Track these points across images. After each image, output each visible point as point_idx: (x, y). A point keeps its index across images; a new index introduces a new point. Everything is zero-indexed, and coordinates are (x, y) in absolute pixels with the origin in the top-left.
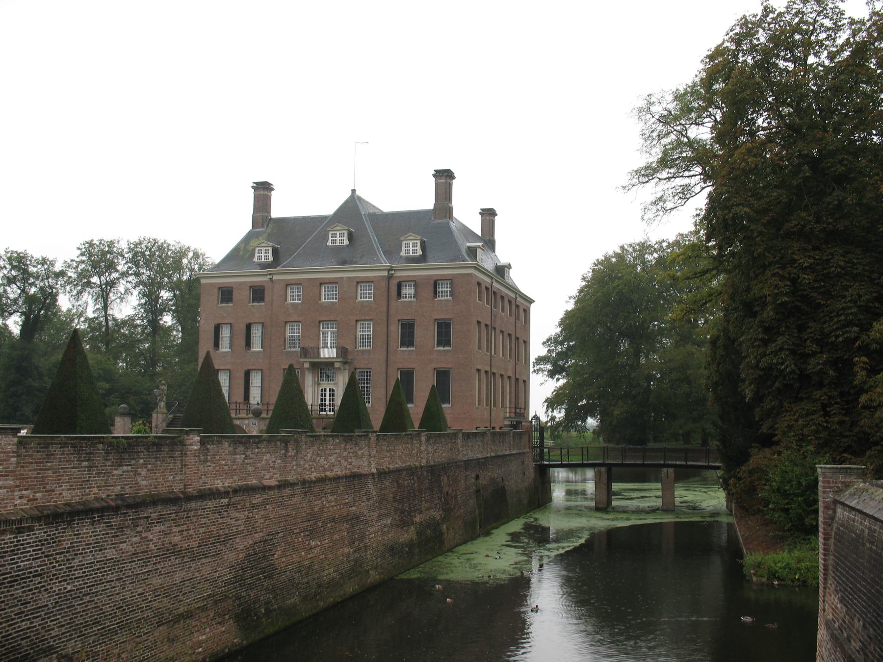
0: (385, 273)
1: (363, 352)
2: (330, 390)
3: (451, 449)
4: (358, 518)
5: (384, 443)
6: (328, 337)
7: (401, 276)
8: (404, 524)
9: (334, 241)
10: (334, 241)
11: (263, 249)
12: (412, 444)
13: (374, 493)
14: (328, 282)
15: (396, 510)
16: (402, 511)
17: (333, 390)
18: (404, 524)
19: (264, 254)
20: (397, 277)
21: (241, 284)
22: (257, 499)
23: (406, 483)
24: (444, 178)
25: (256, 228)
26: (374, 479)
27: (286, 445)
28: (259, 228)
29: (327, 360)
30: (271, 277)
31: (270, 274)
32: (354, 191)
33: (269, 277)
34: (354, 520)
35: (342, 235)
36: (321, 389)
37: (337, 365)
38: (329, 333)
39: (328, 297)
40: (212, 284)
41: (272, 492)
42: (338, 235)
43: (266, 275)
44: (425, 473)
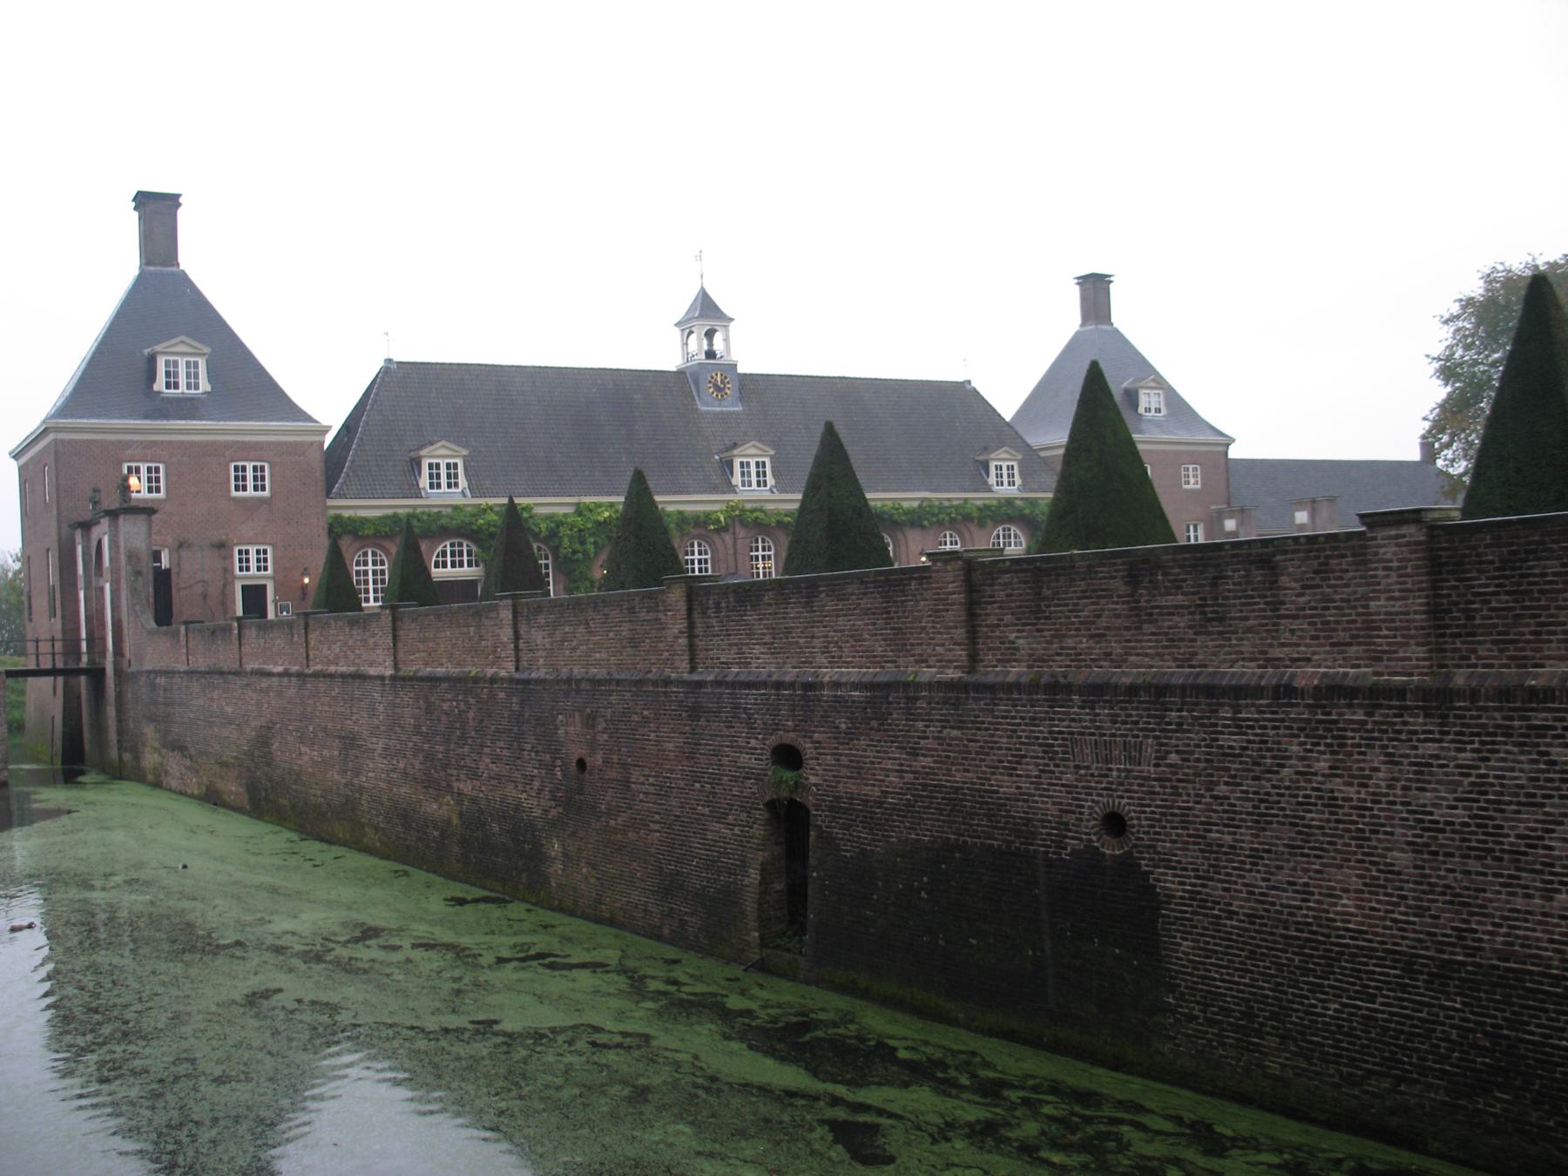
3: (634, 642)
4: (353, 739)
5: (413, 626)
8: (433, 784)
12: (479, 627)
13: (381, 708)
15: (417, 750)
16: (429, 757)
18: (433, 784)
22: (265, 682)
23: (446, 706)
26: (383, 685)
27: (291, 628)
34: (350, 742)
41: (274, 679)
44: (502, 695)
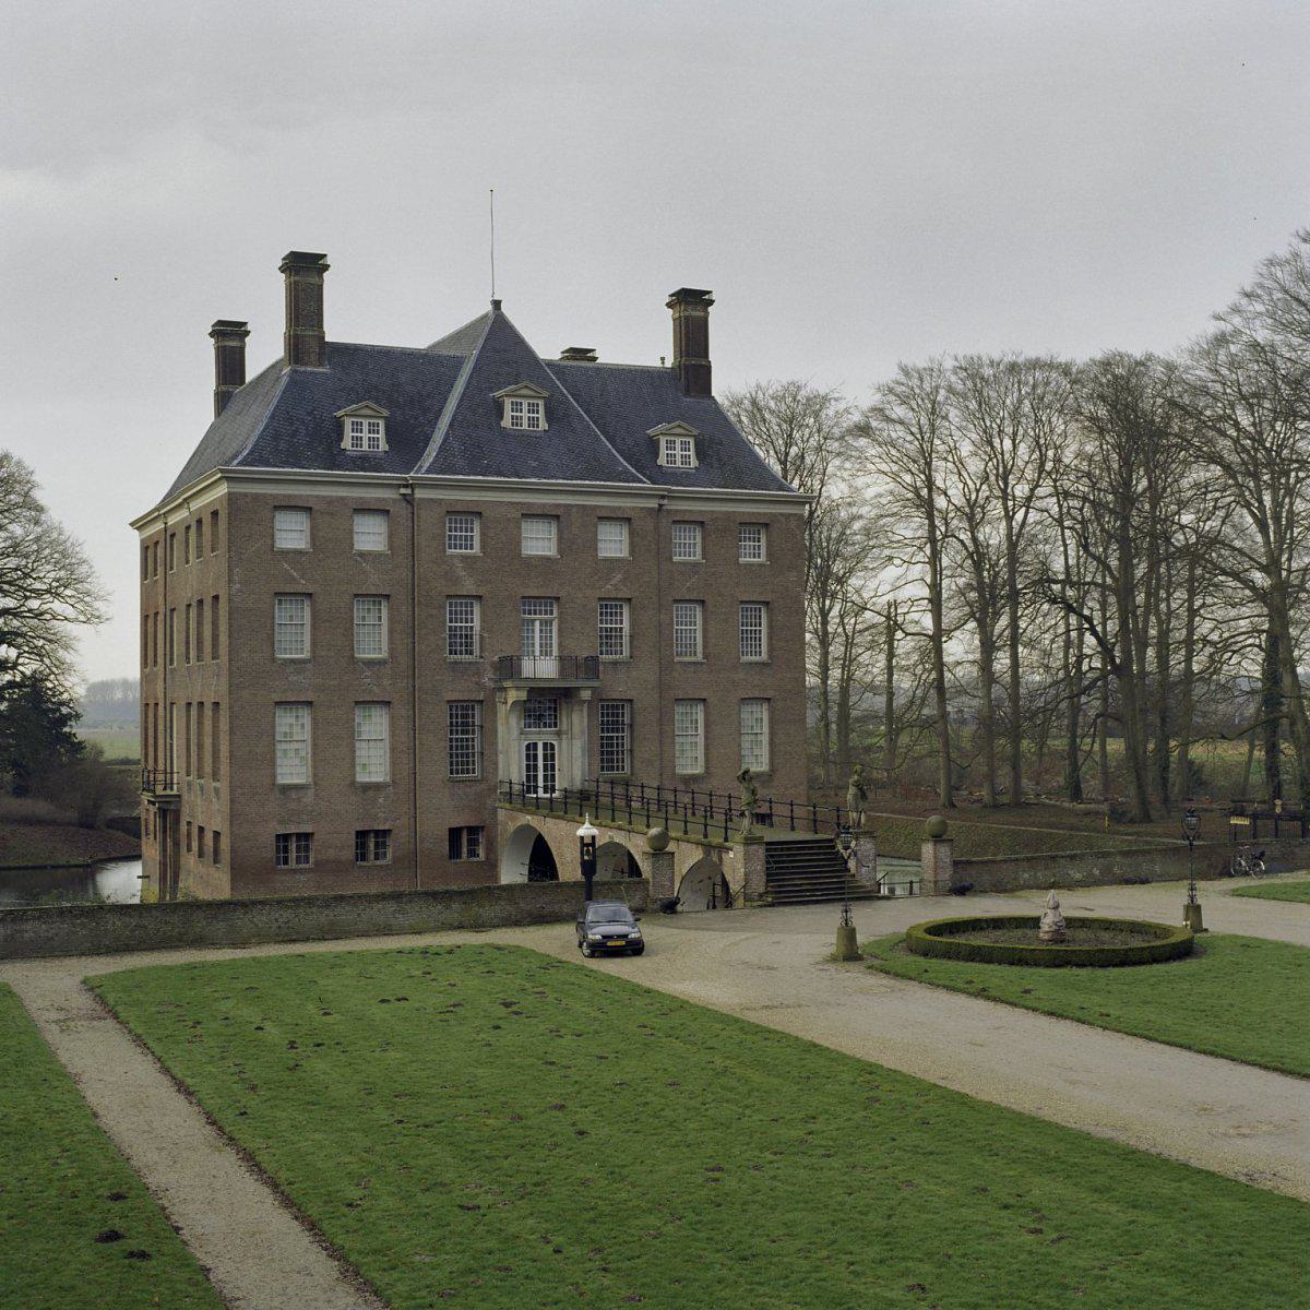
0: (653, 504)
1: (615, 663)
2: (545, 745)
6: (533, 631)
7: (677, 511)
9: (516, 421)
10: (516, 421)
11: (365, 422)
14: (539, 512)
17: (552, 746)
19: (364, 433)
20: (669, 511)
21: (330, 501)
24: (691, 307)
25: (306, 364)
28: (311, 364)
29: (542, 685)
30: (409, 491)
31: (406, 486)
32: (497, 304)
33: (403, 491)
35: (533, 409)
36: (527, 743)
37: (586, 695)
38: (537, 623)
39: (539, 542)
40: (256, 497)
42: (525, 407)
43: (399, 486)
